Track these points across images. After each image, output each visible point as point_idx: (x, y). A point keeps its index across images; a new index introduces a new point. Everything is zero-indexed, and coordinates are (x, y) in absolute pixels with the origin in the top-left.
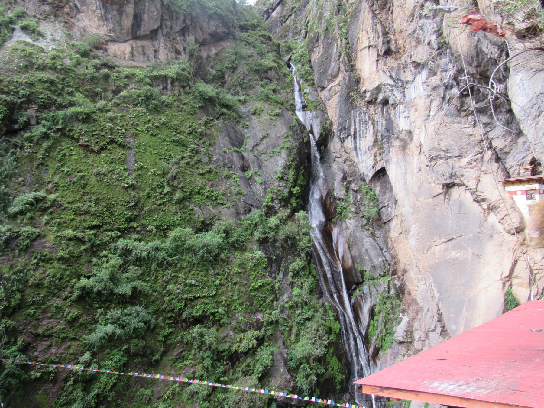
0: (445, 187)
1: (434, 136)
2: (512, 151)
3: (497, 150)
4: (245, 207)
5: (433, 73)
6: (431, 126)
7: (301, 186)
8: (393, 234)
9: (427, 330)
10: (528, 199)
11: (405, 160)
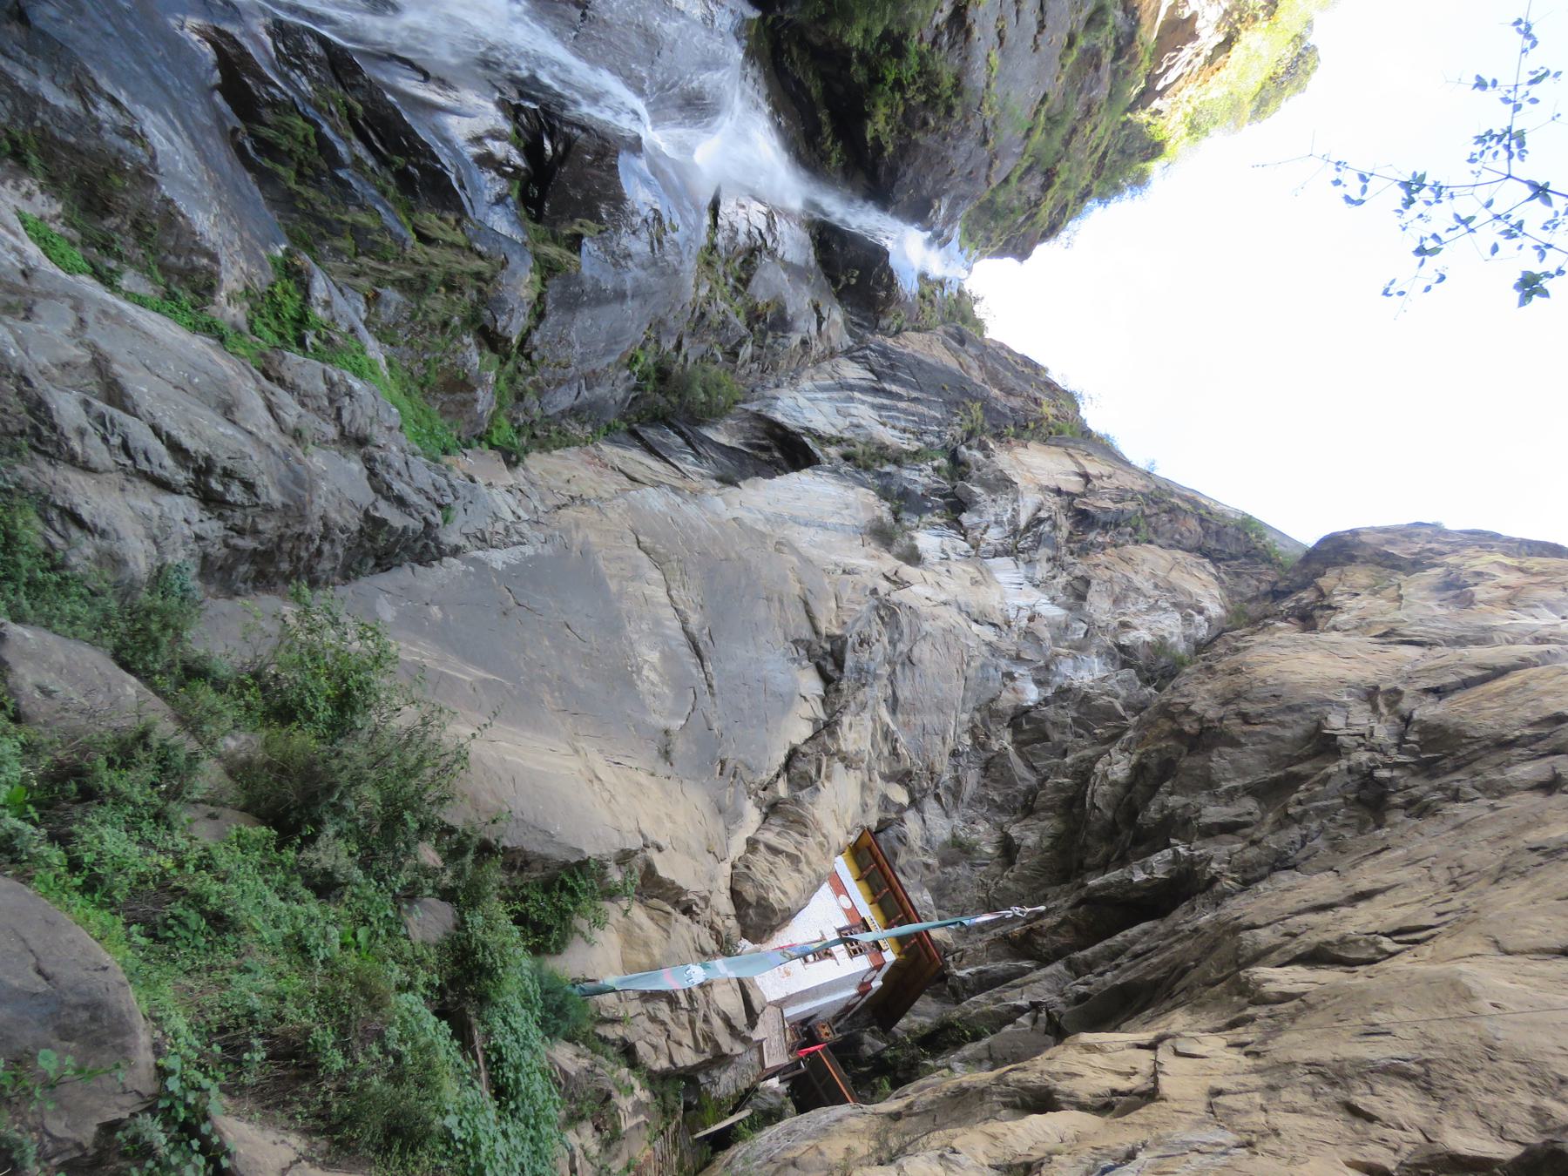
0: (828, 646)
1: (940, 623)
8: (611, 452)
9: (378, 454)
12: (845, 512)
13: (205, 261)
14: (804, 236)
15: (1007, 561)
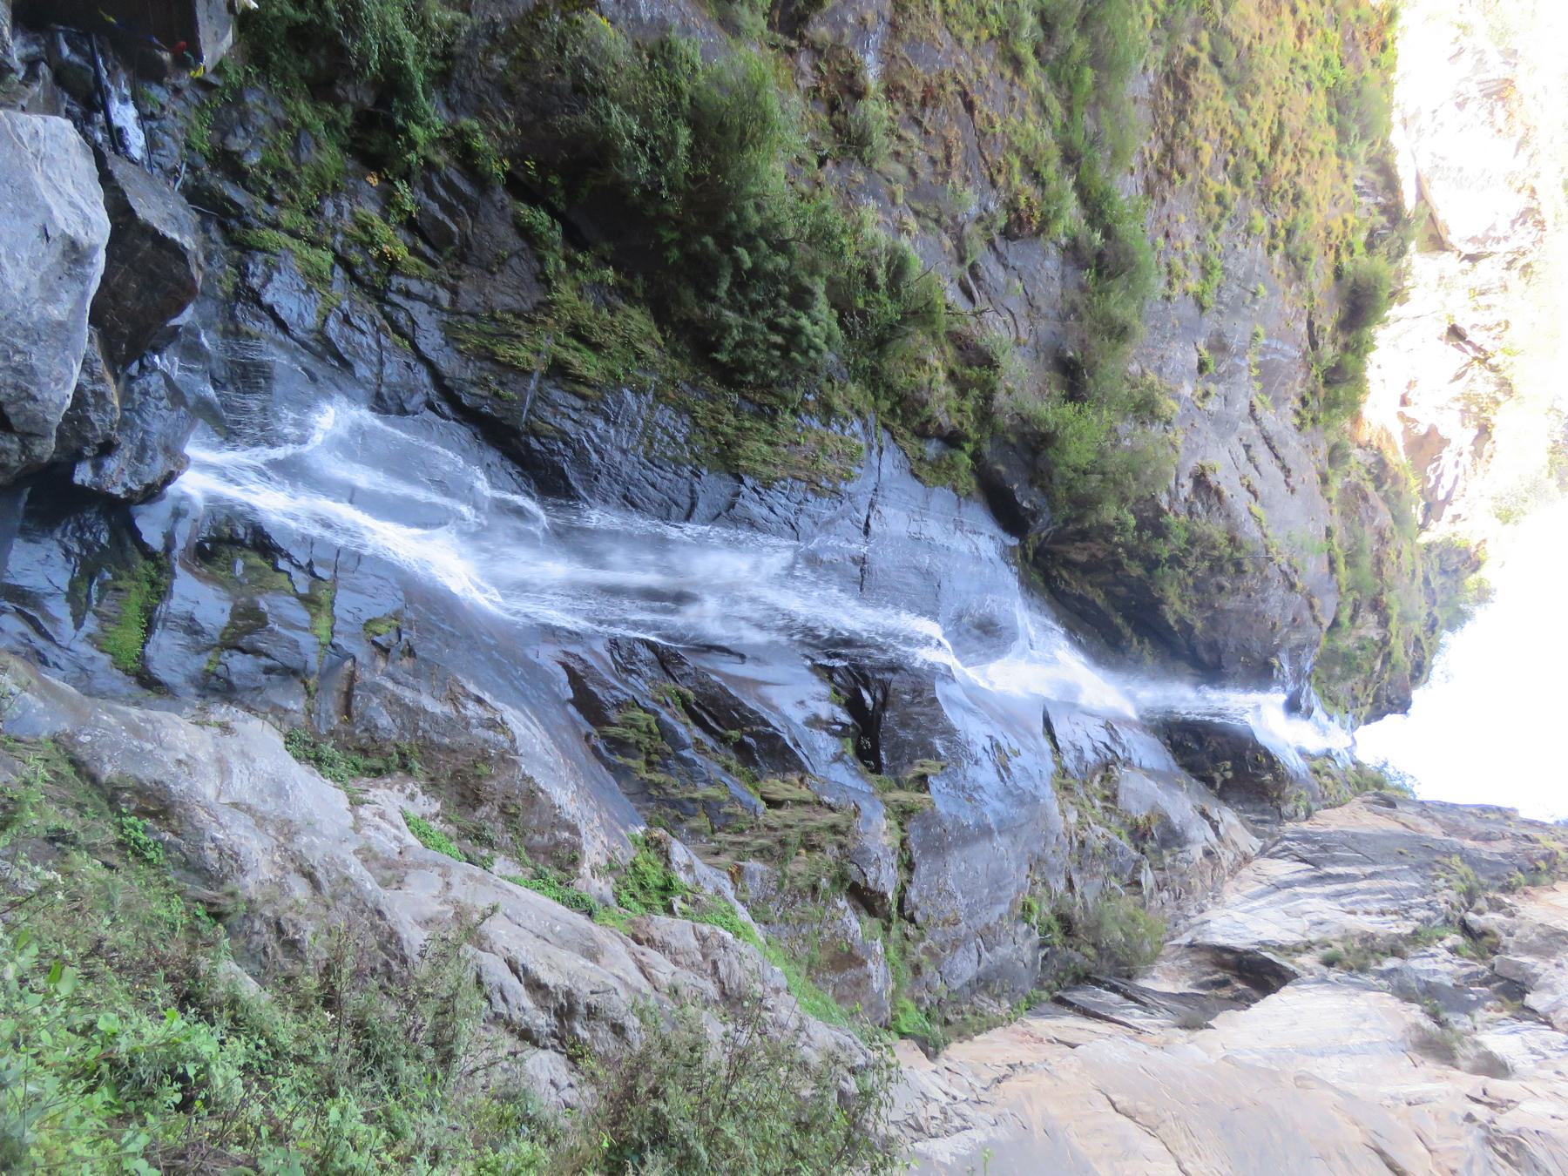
12: (1365, 1026)
13: (566, 834)
14: (1154, 741)
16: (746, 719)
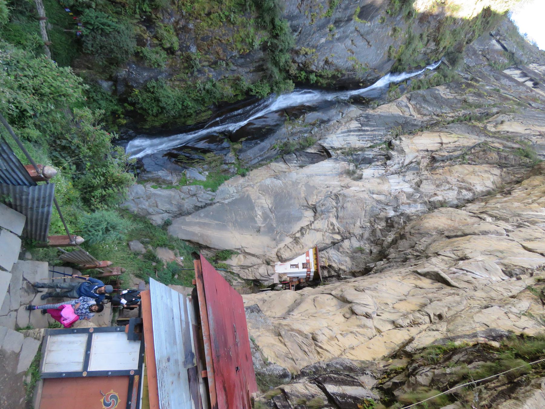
2: (339, 253)
3: (341, 243)
4: (299, 25)
5: (409, 196)
6: (364, 195)
7: (317, 82)
9: (198, 195)
10: (303, 264)
11: (337, 174)
15: (396, 176)
16: (200, 149)
